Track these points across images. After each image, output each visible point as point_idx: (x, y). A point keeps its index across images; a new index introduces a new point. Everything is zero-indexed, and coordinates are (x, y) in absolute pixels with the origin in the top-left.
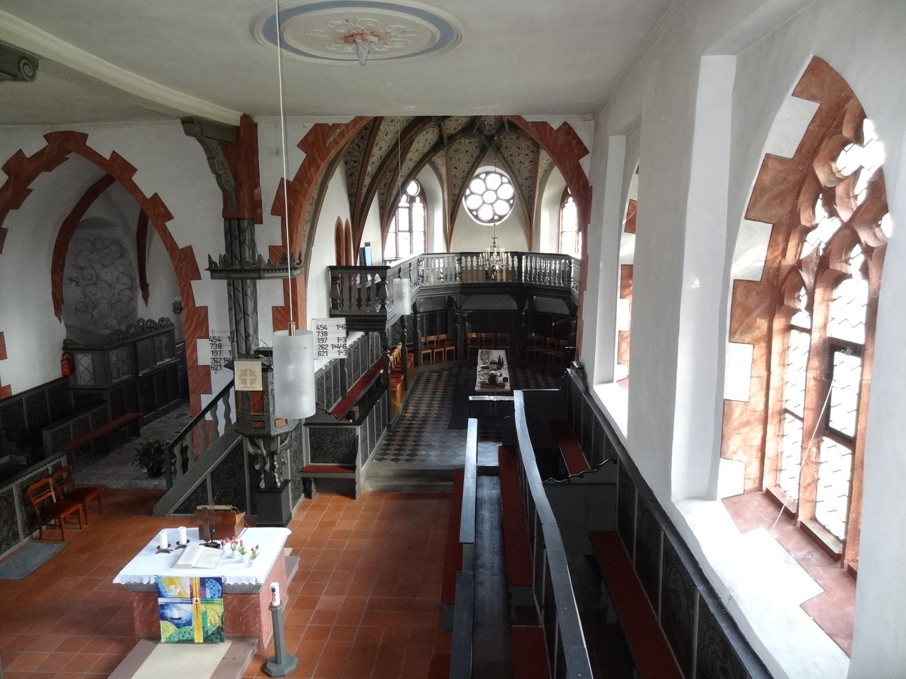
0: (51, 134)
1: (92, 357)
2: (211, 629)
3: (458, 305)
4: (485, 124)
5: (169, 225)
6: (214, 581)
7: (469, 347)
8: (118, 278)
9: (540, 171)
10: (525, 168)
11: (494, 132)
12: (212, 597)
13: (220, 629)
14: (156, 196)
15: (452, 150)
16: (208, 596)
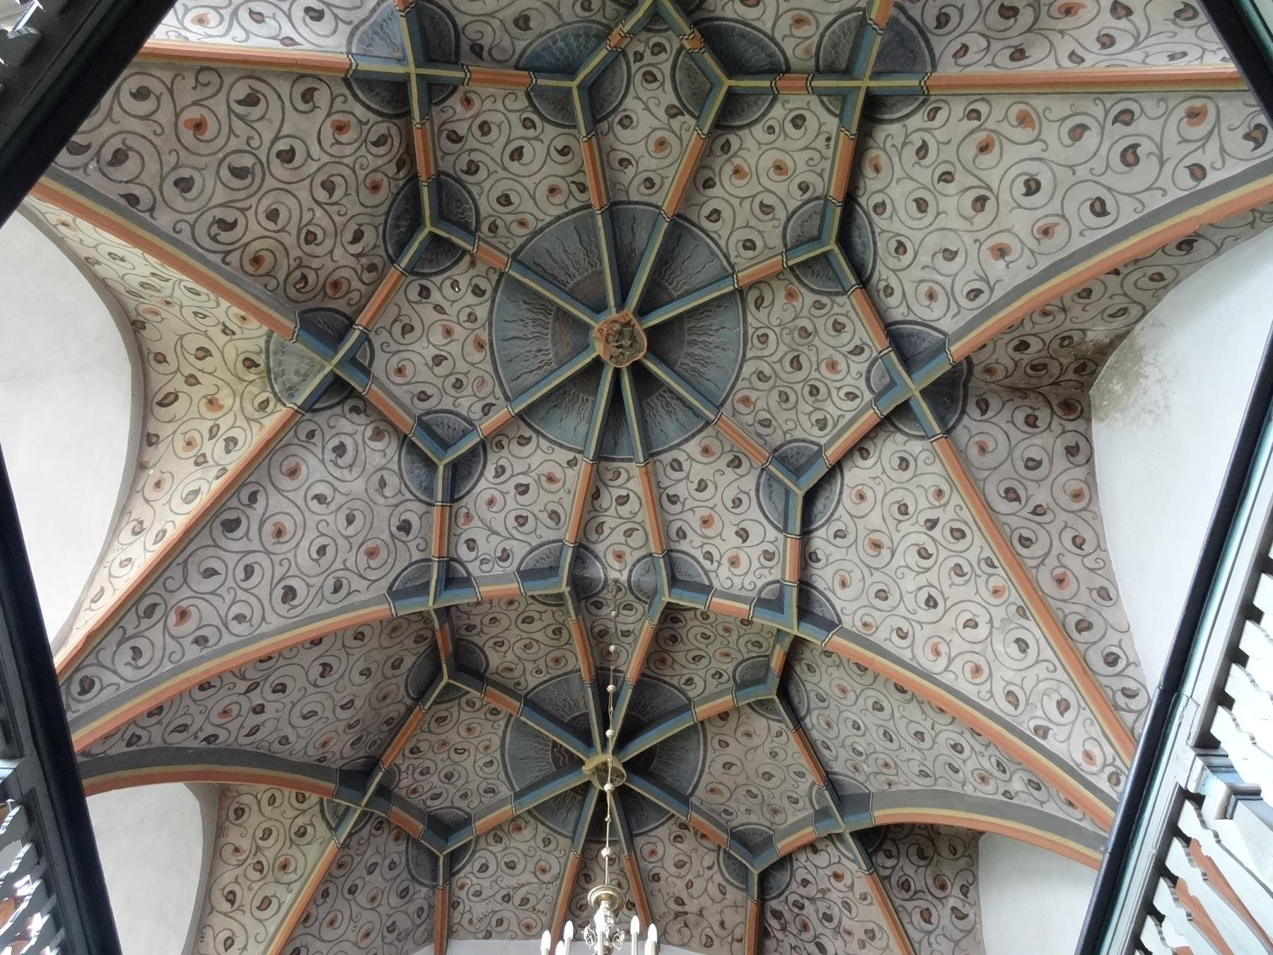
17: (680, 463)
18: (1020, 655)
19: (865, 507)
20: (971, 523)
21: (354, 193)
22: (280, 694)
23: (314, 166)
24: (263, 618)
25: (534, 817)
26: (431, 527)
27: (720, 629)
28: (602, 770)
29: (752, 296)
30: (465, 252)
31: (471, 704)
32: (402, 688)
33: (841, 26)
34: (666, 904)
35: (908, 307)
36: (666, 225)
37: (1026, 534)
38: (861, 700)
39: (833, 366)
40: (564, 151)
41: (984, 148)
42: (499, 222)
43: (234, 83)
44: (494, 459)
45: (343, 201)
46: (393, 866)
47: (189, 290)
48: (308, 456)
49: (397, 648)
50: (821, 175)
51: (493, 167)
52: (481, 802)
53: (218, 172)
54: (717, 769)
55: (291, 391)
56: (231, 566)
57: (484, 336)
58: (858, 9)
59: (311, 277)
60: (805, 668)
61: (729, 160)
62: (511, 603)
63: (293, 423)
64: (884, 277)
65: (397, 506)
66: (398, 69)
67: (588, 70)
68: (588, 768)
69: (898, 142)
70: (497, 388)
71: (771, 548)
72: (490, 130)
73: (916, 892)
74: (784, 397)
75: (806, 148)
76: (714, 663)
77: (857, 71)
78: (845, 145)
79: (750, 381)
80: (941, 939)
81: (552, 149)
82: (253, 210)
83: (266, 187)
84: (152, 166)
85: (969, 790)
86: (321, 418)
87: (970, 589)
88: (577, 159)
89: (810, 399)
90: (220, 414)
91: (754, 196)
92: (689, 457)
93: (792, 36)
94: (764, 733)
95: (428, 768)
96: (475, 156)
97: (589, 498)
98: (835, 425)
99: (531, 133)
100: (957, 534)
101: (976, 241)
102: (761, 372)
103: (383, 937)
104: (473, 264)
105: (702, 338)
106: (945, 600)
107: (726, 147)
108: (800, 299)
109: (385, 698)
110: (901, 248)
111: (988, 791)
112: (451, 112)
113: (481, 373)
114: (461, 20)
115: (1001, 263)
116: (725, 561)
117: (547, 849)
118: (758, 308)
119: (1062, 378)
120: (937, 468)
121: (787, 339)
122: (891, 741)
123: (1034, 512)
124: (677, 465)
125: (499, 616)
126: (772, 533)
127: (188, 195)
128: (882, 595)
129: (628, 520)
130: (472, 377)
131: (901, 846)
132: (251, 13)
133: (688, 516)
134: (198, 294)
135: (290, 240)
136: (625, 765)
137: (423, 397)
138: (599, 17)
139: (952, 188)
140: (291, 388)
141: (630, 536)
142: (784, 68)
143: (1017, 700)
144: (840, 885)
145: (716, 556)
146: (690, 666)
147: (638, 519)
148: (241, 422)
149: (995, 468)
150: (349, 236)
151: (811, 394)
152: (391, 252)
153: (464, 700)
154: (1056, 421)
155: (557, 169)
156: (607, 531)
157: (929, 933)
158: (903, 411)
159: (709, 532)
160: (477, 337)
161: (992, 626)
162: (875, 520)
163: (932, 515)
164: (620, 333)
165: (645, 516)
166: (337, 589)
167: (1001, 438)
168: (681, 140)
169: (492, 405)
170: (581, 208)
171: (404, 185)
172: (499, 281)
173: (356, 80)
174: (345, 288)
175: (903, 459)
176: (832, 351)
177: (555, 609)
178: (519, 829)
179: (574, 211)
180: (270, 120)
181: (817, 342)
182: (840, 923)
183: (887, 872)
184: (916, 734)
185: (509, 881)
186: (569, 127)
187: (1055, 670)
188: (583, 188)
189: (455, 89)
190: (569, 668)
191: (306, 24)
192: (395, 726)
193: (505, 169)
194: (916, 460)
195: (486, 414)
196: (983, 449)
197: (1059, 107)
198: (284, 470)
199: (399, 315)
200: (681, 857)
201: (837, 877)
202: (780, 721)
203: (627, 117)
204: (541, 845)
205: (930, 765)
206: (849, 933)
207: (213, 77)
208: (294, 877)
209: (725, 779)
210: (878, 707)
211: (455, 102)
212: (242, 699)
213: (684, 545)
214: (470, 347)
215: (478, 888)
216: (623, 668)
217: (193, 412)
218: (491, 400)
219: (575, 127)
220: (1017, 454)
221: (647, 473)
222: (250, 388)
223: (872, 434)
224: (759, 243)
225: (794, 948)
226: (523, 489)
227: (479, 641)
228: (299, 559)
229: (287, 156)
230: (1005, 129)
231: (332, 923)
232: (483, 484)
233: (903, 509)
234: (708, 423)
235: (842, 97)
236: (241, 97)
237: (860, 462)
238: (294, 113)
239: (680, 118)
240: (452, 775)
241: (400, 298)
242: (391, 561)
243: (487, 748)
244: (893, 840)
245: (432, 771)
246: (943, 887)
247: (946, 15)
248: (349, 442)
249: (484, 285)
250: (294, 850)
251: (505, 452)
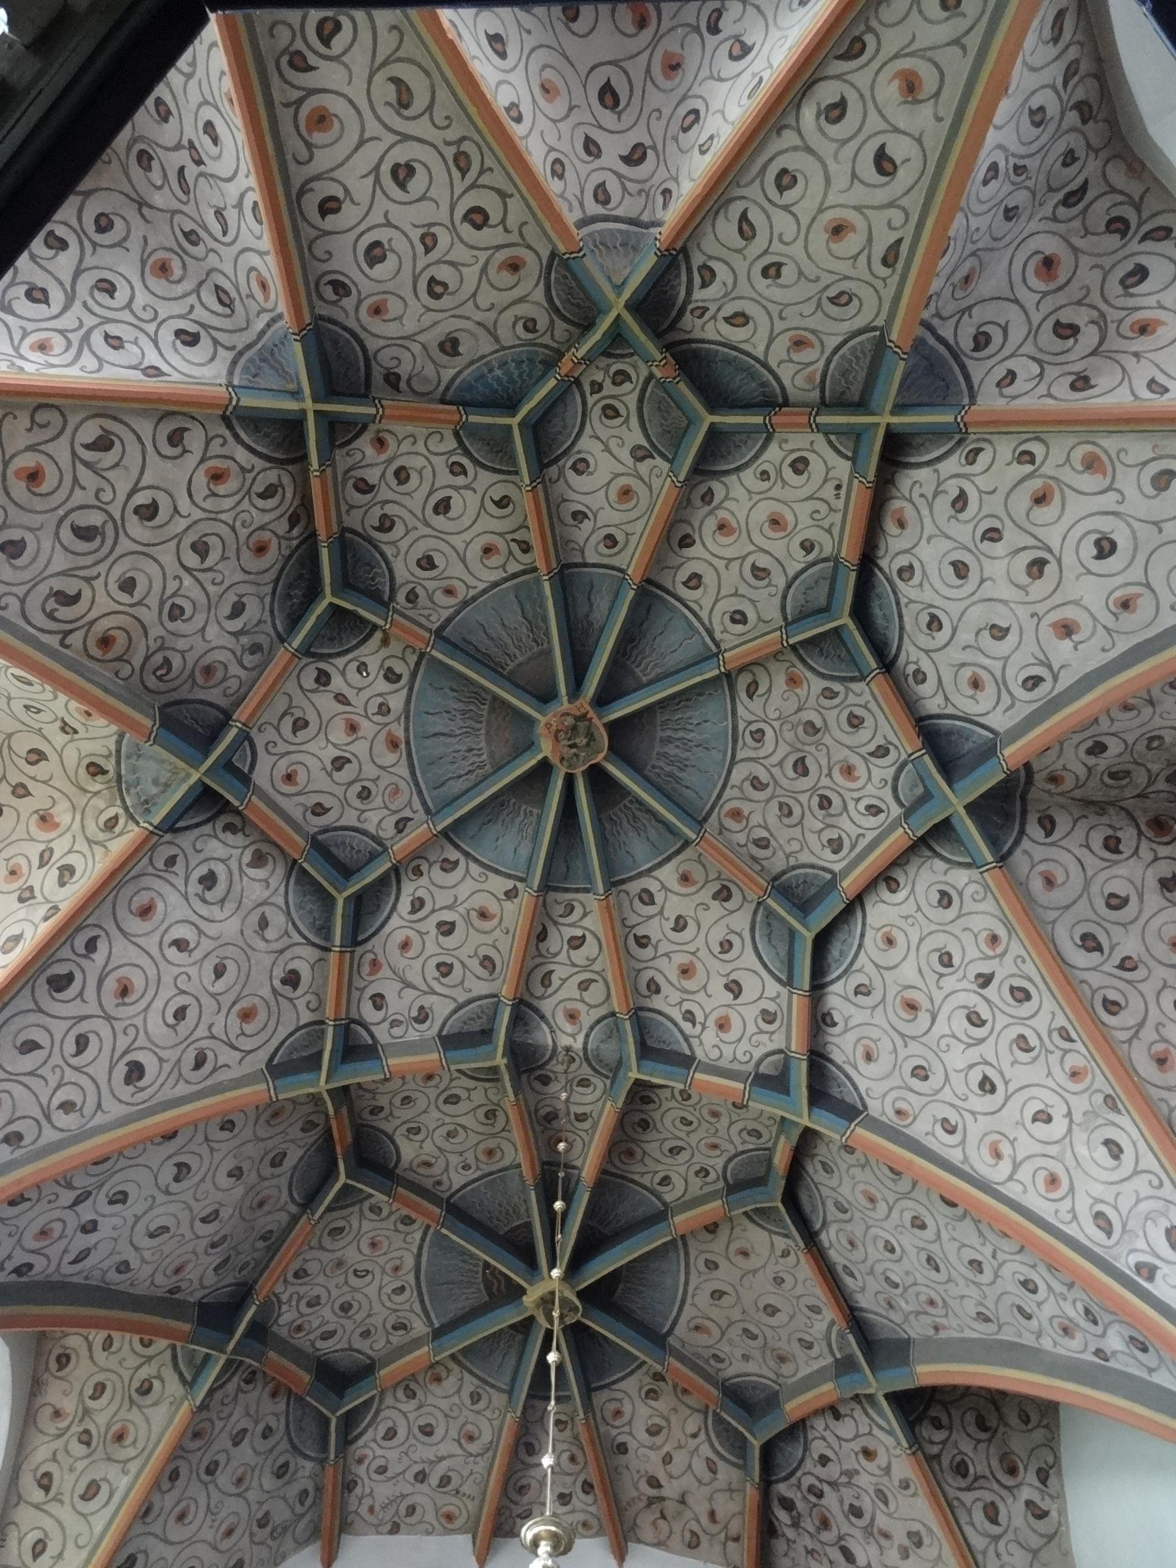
10: (361, 143)
17: (651, 895)
18: (1112, 1163)
19: (895, 955)
20: (1038, 980)
21: (233, 556)
22: (118, 1207)
23: (182, 524)
24: (99, 1106)
25: (459, 1363)
26: (326, 979)
27: (705, 1112)
28: (547, 1302)
29: (743, 682)
30: (375, 627)
31: (376, 1209)
32: (285, 1191)
33: (853, 350)
34: (637, 1489)
35: (946, 698)
36: (632, 593)
37: (1112, 995)
38: (895, 1214)
39: (848, 771)
40: (502, 503)
41: (1040, 499)
42: (419, 590)
43: (82, 423)
44: (409, 889)
45: (219, 567)
46: (267, 1433)
47: (18, 678)
48: (166, 889)
49: (279, 1138)
50: (829, 531)
51: (411, 522)
52: (388, 1342)
53: (57, 534)
54: (703, 1299)
55: (147, 805)
56: (58, 1037)
57: (400, 733)
58: (874, 329)
59: (176, 662)
60: (819, 1167)
61: (711, 513)
62: (430, 1077)
63: (147, 848)
64: (913, 658)
65: (281, 952)
66: (292, 405)
67: (532, 404)
68: (531, 1298)
69: (929, 492)
70: (415, 798)
71: (771, 1007)
72: (408, 478)
73: (976, 1479)
74: (786, 811)
75: (810, 498)
76: (698, 1158)
77: (873, 405)
78: (860, 497)
79: (741, 788)
80: (1013, 1547)
81: (487, 500)
82: (102, 578)
83: (118, 551)
85: (1046, 1344)
86: (185, 840)
87: (1040, 1065)
88: (518, 510)
89: (820, 814)
90: (54, 834)
91: (744, 558)
92: (664, 887)
93: (791, 361)
94: (766, 1252)
95: (318, 1297)
96: (390, 509)
97: (534, 940)
98: (853, 847)
99: (460, 480)
100: (1020, 995)
101: (1032, 616)
102: (756, 778)
103: (252, 1535)
104: (385, 642)
105: (681, 734)
106: (1006, 1083)
107: (708, 497)
108: (805, 686)
109: (261, 1204)
110: (934, 623)
111: (1073, 1348)
112: (358, 456)
113: (395, 779)
114: (372, 345)
115: (1067, 644)
116: (711, 1023)
117: (476, 1407)
118: (750, 697)
119: (1150, 790)
120: (989, 905)
121: (789, 736)
122: (937, 1269)
123: (1121, 966)
124: (647, 898)
125: (414, 1095)
126: (773, 988)
127: (18, 562)
128: (921, 1073)
129: (585, 969)
130: (382, 784)
131: (953, 1412)
132: (107, 337)
133: (662, 963)
134: (30, 684)
135: (149, 616)
136: (580, 1294)
137: (319, 810)
138: (546, 340)
139: (999, 548)
140: (146, 802)
141: (586, 989)
142: (780, 400)
143: (1110, 1223)
144: (870, 1466)
145: (700, 1018)
146: (665, 1160)
147: (597, 967)
148: (81, 845)
149: (1067, 907)
150: (226, 609)
151: (821, 807)
152: (280, 628)
153: (367, 1204)
154: (1144, 845)
155: (494, 523)
156: (555, 980)
157: (996, 1538)
158: (943, 830)
159: (689, 985)
160: (389, 733)
161: (1071, 1121)
162: (908, 972)
163: (985, 967)
164: (574, 728)
165: (605, 963)
166: (199, 1063)
167: (1074, 868)
168: (650, 488)
169: (410, 819)
170: (524, 572)
171: (298, 547)
172: (418, 664)
173: (238, 418)
174: (219, 674)
175: (943, 894)
176: (847, 752)
177: (487, 1085)
178: (438, 1379)
179: (515, 576)
180: (126, 468)
181: (827, 740)
182: (873, 1520)
183: (935, 1450)
184: (971, 1262)
185: (424, 1452)
186: (509, 473)
187: (1161, 1184)
188: (526, 548)
189: (365, 427)
190: (507, 1162)
191: (176, 350)
192: (274, 1242)
193: (427, 524)
194: (961, 895)
195: (400, 831)
196: (1049, 882)
197: (1138, 449)
198: (133, 908)
199: (290, 707)
200: (657, 1420)
201: (868, 1454)
202: (786, 1236)
203: (584, 460)
204: (468, 1401)
205: (991, 1306)
206: (886, 1536)
207: (55, 418)
208: (131, 1452)
209: (714, 1313)
210: (918, 1224)
211: (365, 444)
212: (68, 1215)
213: (657, 1002)
214: (381, 746)
215: (382, 1462)
216: (578, 1163)
217: (20, 832)
218: (407, 813)
219: (516, 473)
220: (1095, 888)
221: (608, 907)
222: (94, 802)
223: (901, 860)
224: (751, 615)
225: (810, 1552)
226: (447, 929)
227: (388, 1127)
228: (151, 1027)
229: (148, 512)
230: (1067, 475)
231: (181, 1517)
232: (395, 921)
233: (946, 960)
234: (687, 843)
235: (856, 435)
236: (90, 440)
237: (885, 894)
238: (157, 458)
239: (648, 461)
240: (351, 1306)
241: (291, 686)
242: (272, 1025)
243: (397, 1269)
244: (944, 1405)
245: (323, 1301)
246: (1012, 1471)
247: (986, 334)
248: (220, 870)
249: (399, 667)
250: (135, 1416)
251: (424, 881)
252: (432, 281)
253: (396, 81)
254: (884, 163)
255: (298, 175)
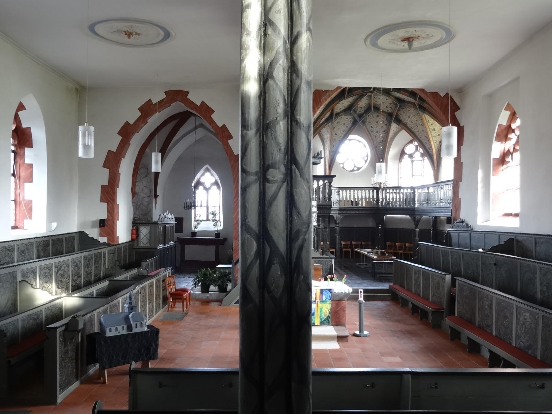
0: (168, 91)
1: (150, 229)
2: (324, 318)
3: (337, 222)
4: (358, 107)
5: (230, 141)
6: (327, 291)
7: (344, 250)
8: (143, 190)
9: (390, 137)
11: (363, 112)
12: (326, 300)
13: (328, 317)
14: (224, 126)
15: (335, 123)
16: (324, 299)
84: (424, 134)
96: (389, 105)
229: (411, 122)
252: (377, 123)
253: (376, 138)
254: (336, 134)
255: (386, 134)
